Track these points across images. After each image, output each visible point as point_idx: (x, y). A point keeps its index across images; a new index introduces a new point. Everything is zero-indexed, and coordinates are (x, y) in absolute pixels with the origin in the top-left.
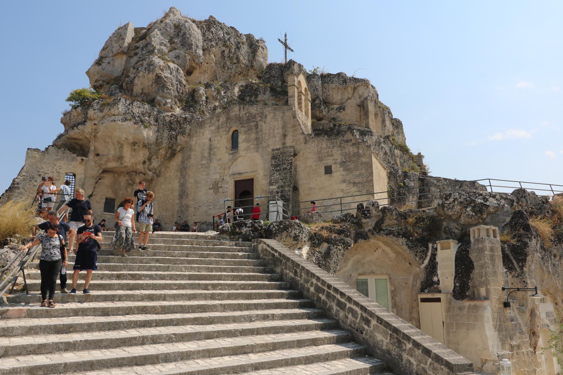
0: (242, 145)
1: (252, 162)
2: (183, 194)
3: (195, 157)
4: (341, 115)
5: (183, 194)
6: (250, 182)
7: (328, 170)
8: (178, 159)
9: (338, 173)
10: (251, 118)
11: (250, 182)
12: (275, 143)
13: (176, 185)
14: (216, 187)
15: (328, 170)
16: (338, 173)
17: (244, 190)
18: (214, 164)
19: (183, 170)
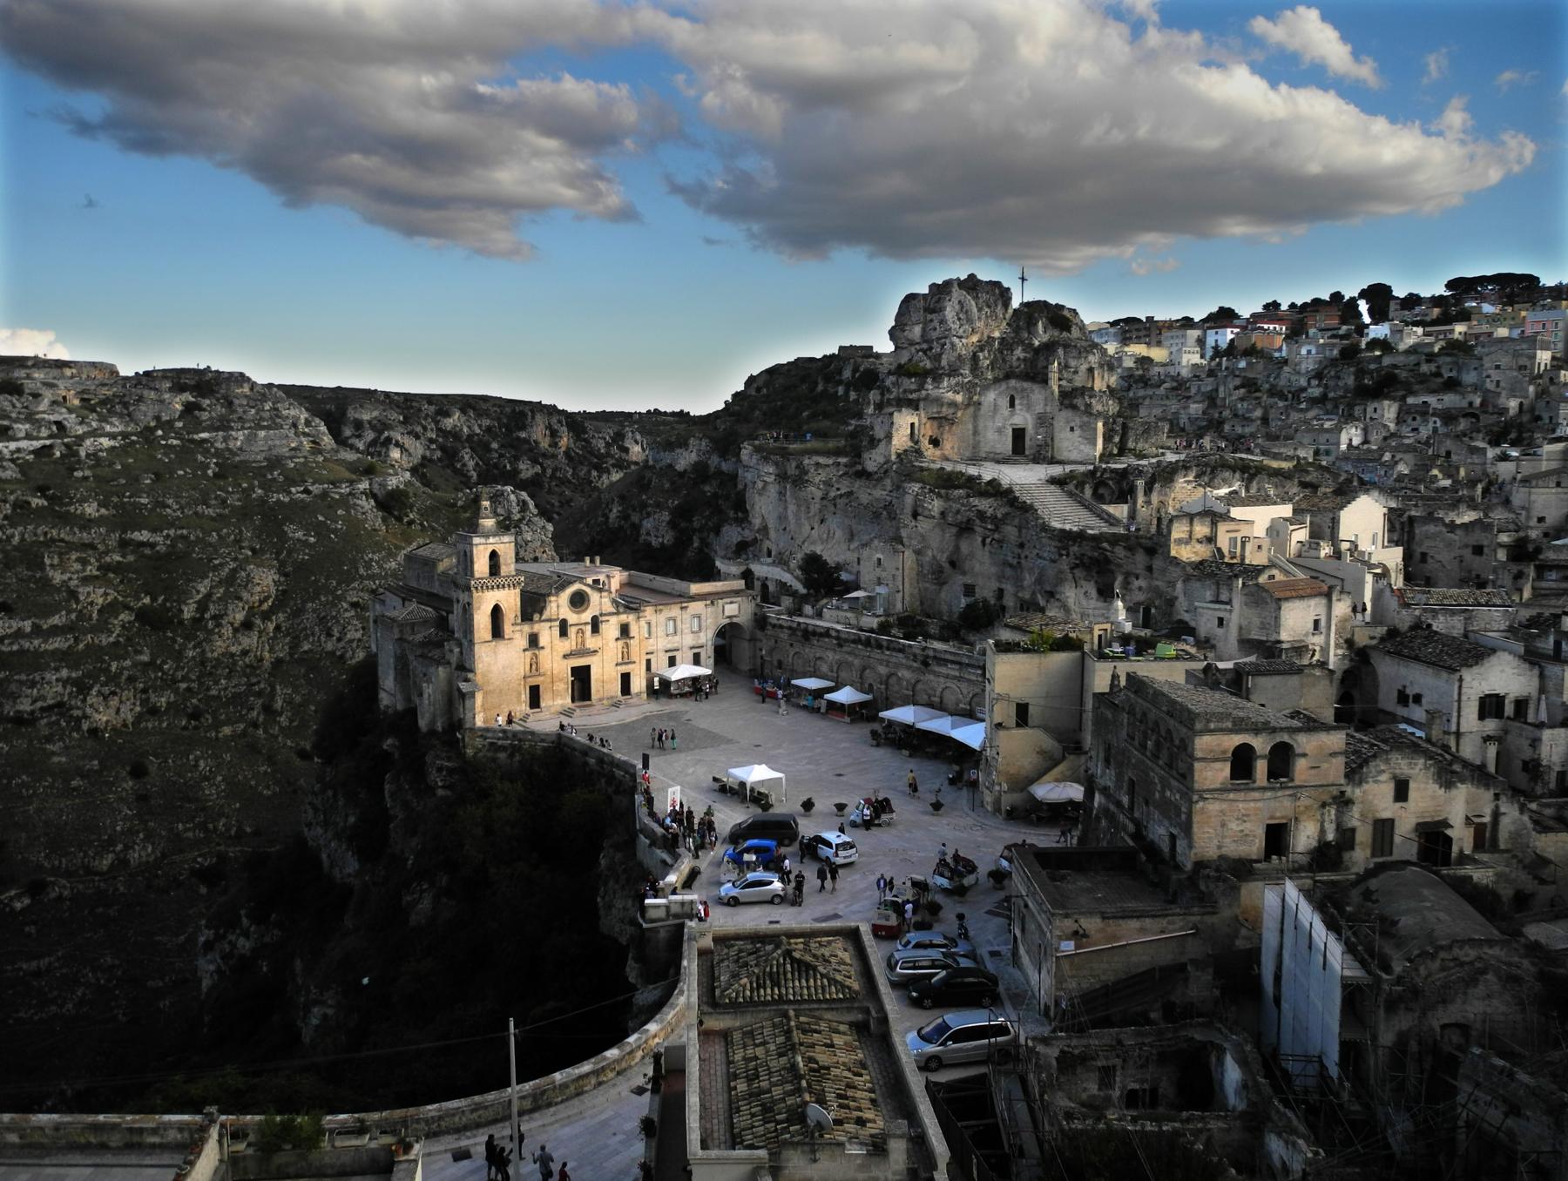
0: (1018, 407)
1: (1023, 418)
2: (976, 433)
3: (984, 409)
4: (1076, 377)
5: (976, 433)
6: (1023, 430)
7: (1072, 429)
8: (971, 409)
9: (1078, 432)
10: (1023, 390)
11: (1023, 430)
12: (1039, 409)
13: (970, 426)
14: (1000, 431)
15: (1072, 429)
16: (1078, 432)
17: (1019, 434)
18: (998, 417)
19: (975, 417)
